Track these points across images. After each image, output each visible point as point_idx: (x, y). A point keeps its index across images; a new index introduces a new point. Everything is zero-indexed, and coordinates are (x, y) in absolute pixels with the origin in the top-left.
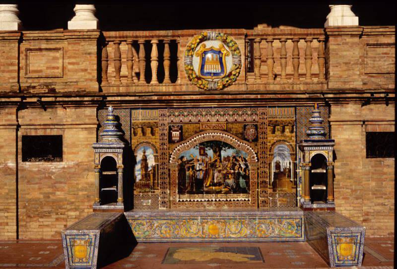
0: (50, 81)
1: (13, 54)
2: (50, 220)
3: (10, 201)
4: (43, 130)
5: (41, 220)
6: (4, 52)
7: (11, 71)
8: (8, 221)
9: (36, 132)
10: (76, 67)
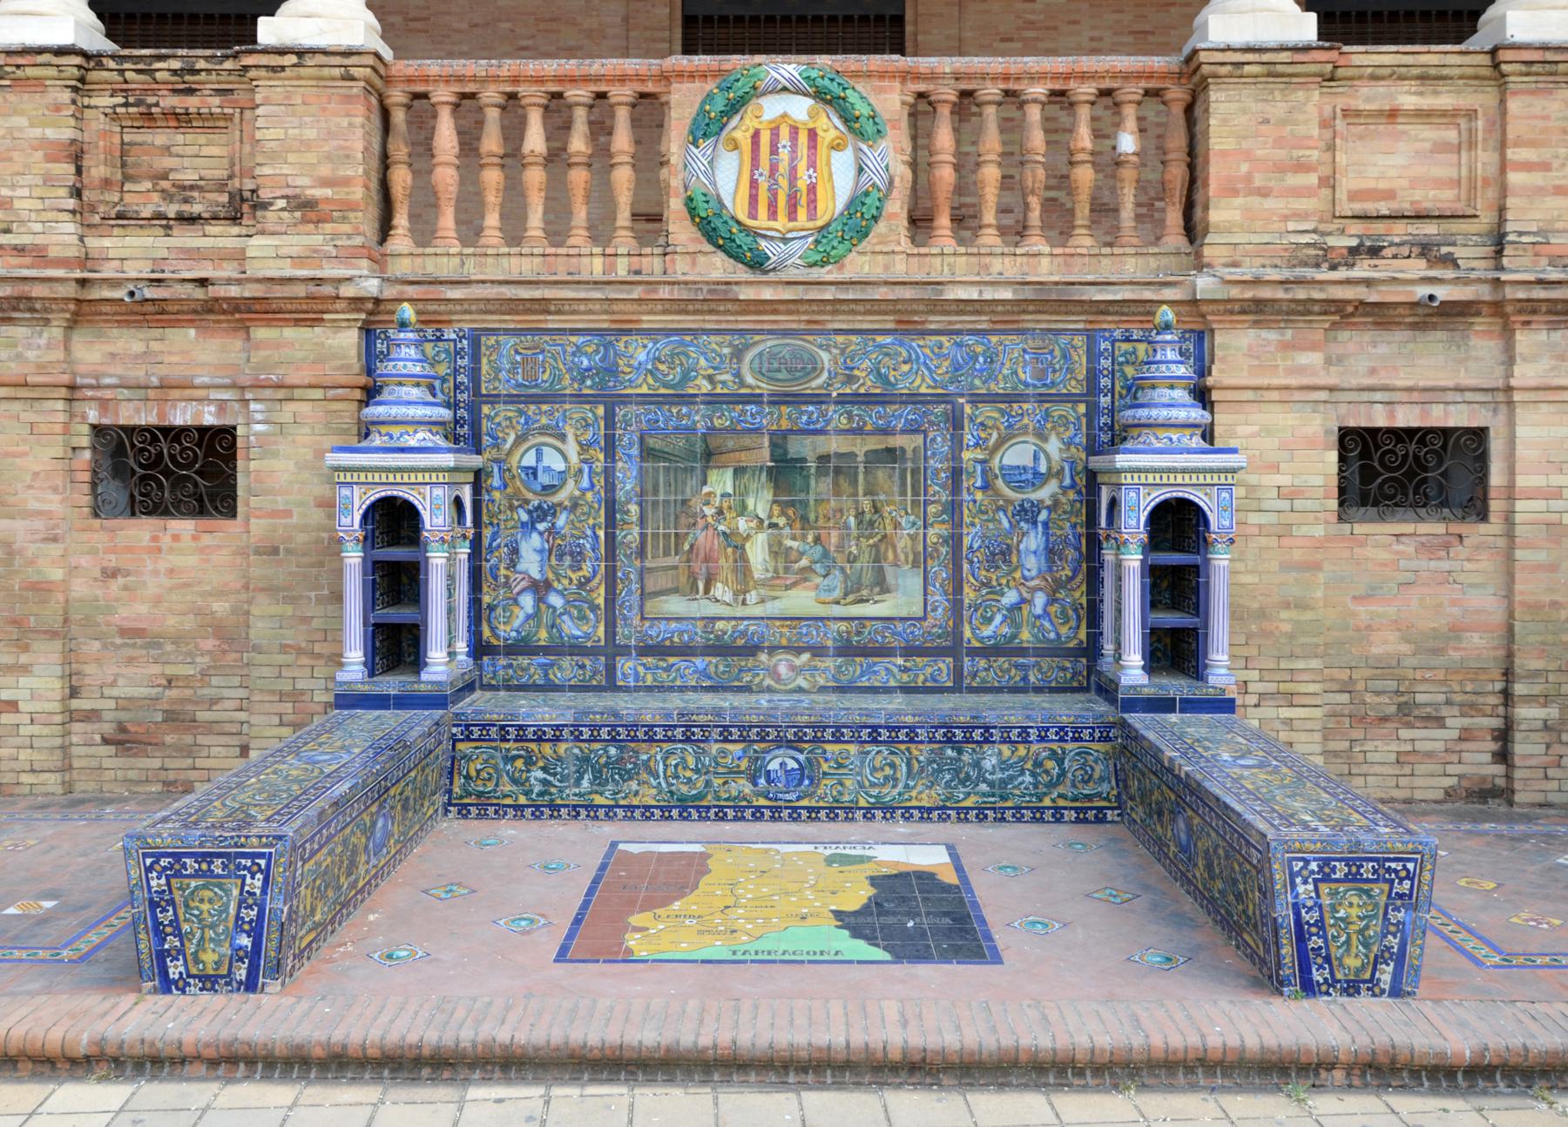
0: (1430, 229)
1: (1301, 130)
2: (1439, 733)
3: (1300, 665)
4: (1417, 409)
5: (1405, 733)
6: (1266, 121)
7: (1297, 192)
8: (1294, 736)
9: (1392, 415)
10: (1537, 178)
